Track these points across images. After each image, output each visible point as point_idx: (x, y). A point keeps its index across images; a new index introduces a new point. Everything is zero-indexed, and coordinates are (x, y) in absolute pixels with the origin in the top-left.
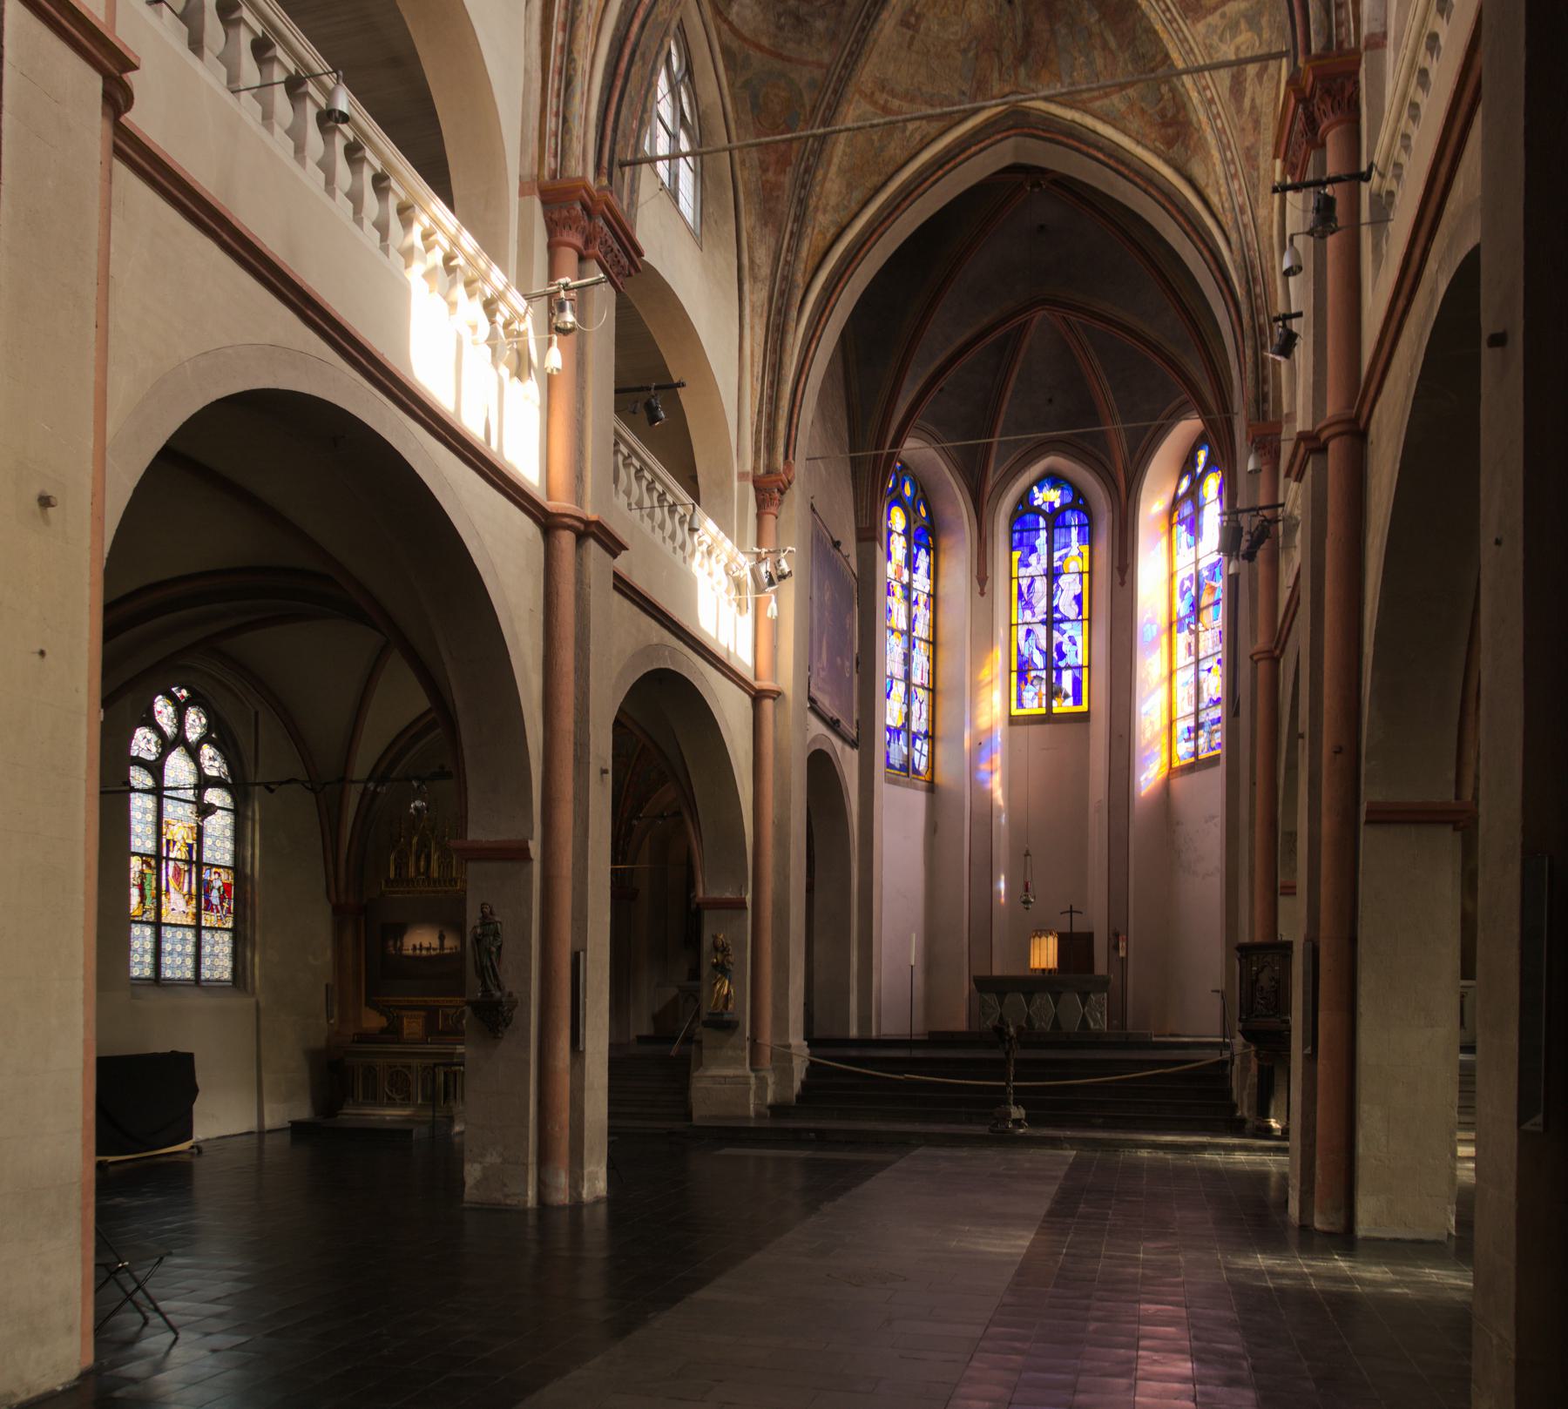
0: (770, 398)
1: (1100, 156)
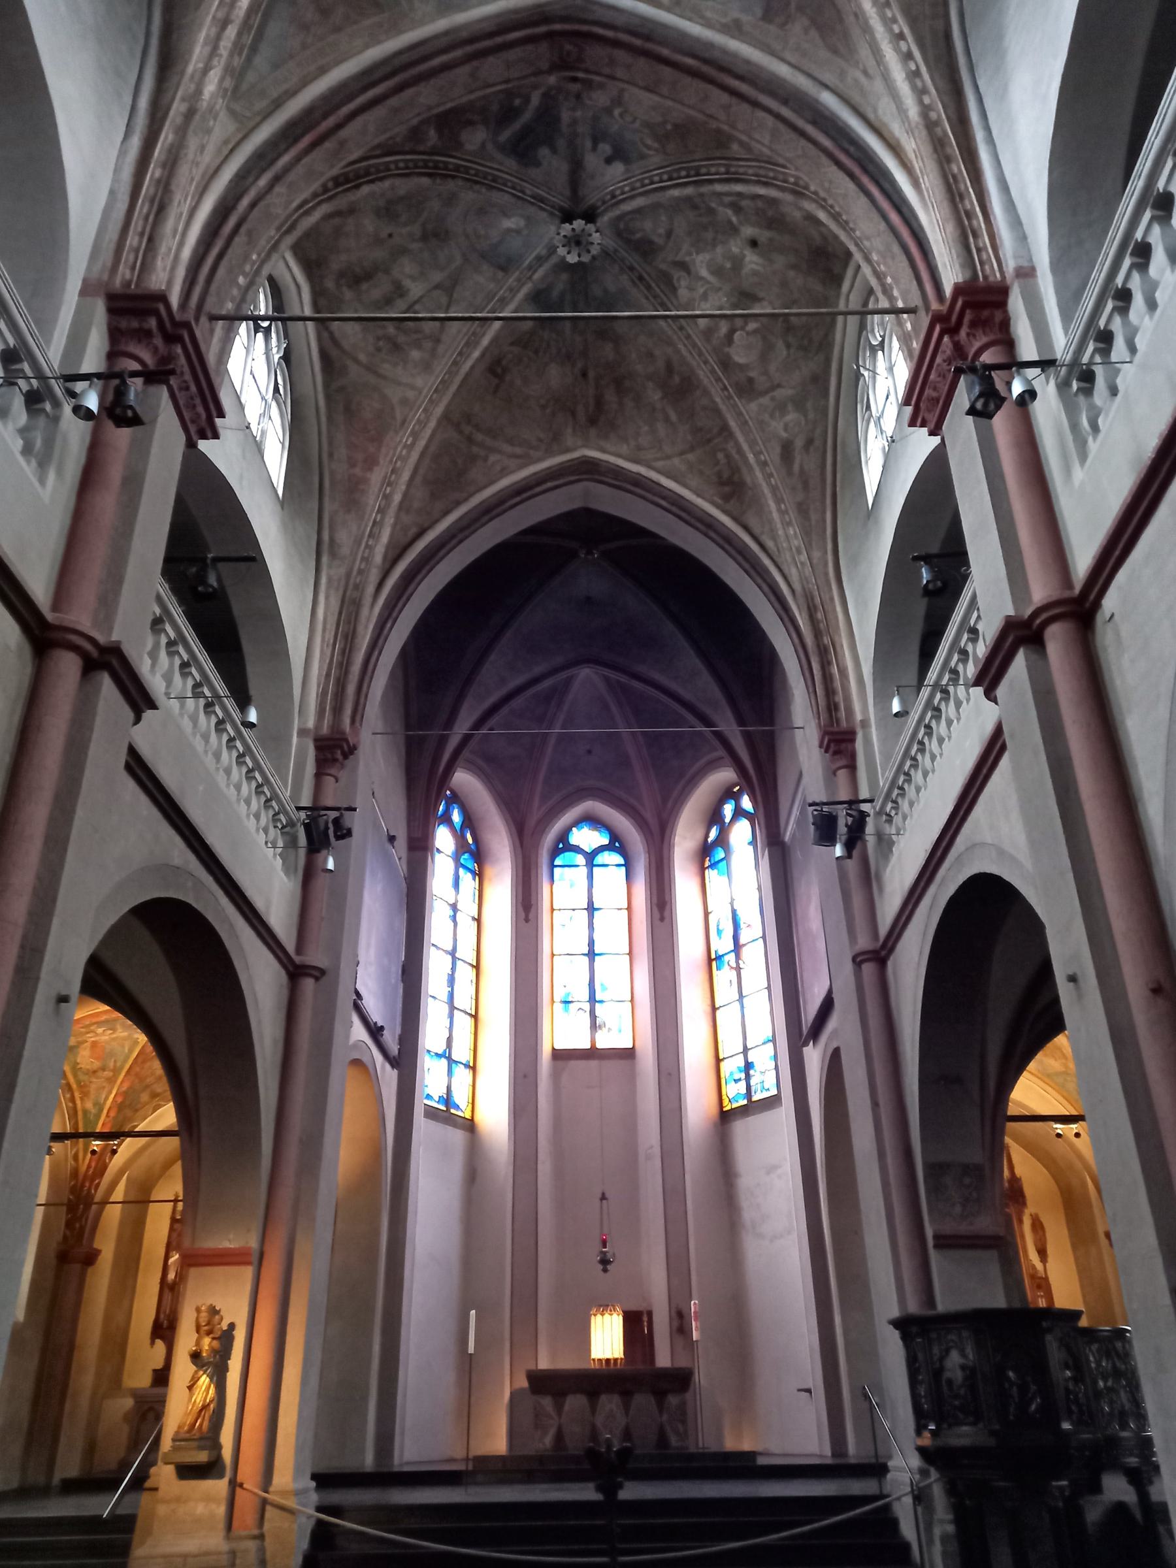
0: (340, 664)
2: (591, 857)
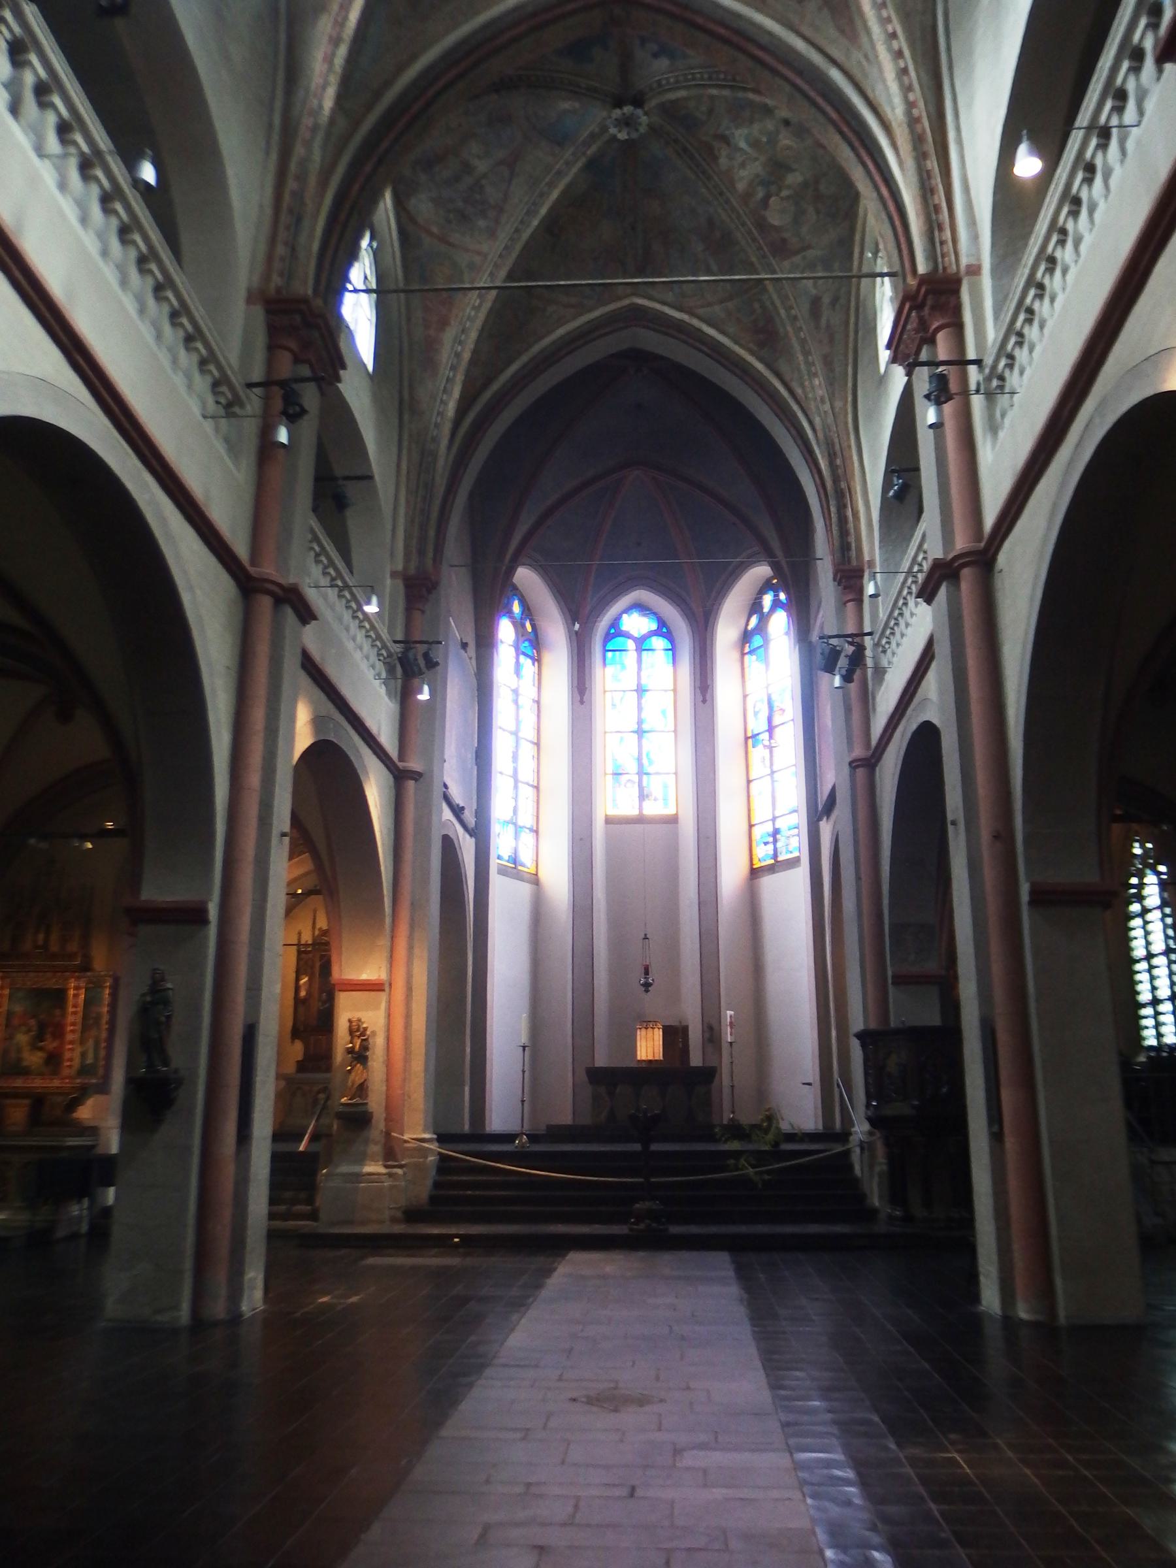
1: (705, 349)
2: (641, 643)
